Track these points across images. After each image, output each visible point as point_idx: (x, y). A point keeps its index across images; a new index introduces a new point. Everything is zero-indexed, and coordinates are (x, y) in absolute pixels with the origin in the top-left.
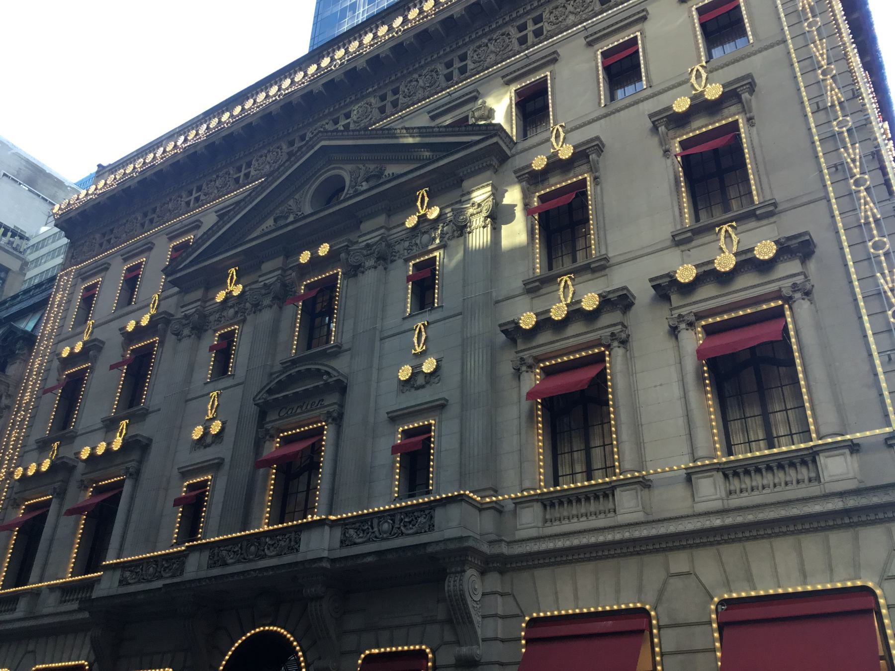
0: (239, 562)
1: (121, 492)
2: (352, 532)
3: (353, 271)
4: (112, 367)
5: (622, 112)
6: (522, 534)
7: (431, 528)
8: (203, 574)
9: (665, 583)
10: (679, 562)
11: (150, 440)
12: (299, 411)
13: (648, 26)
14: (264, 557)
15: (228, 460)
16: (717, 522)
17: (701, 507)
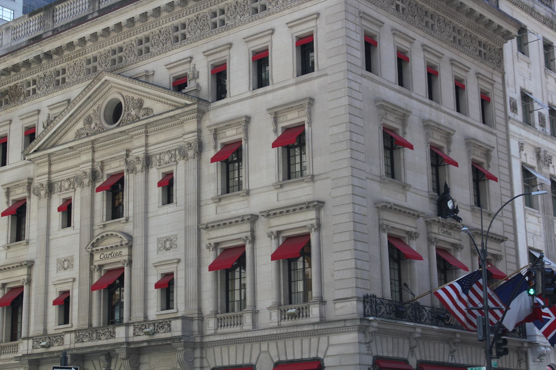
0: (89, 341)
1: (23, 293)
2: (137, 330)
3: (133, 170)
4: (3, 214)
5: (259, 97)
6: (208, 332)
7: (170, 331)
8: (72, 346)
9: (259, 355)
10: (264, 346)
11: (34, 262)
12: (110, 256)
13: (275, 37)
14: (100, 339)
15: (77, 279)
16: (275, 332)
17: (272, 325)
